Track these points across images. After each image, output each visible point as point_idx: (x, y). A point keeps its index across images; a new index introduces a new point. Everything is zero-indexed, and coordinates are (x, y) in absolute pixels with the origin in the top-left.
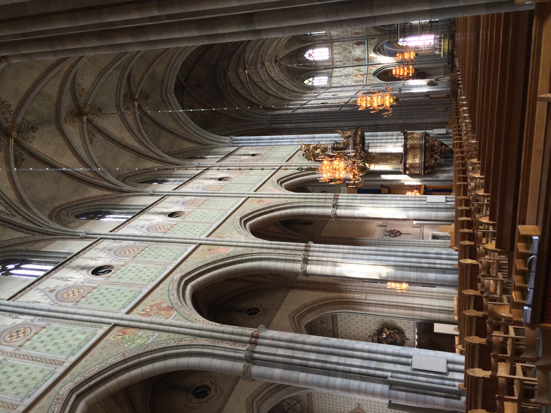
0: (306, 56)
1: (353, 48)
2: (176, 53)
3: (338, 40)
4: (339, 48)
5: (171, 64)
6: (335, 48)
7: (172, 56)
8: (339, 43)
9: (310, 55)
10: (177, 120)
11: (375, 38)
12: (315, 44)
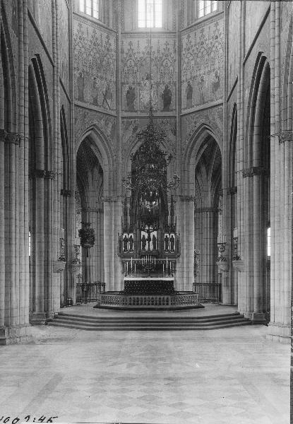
11: (175, 134)
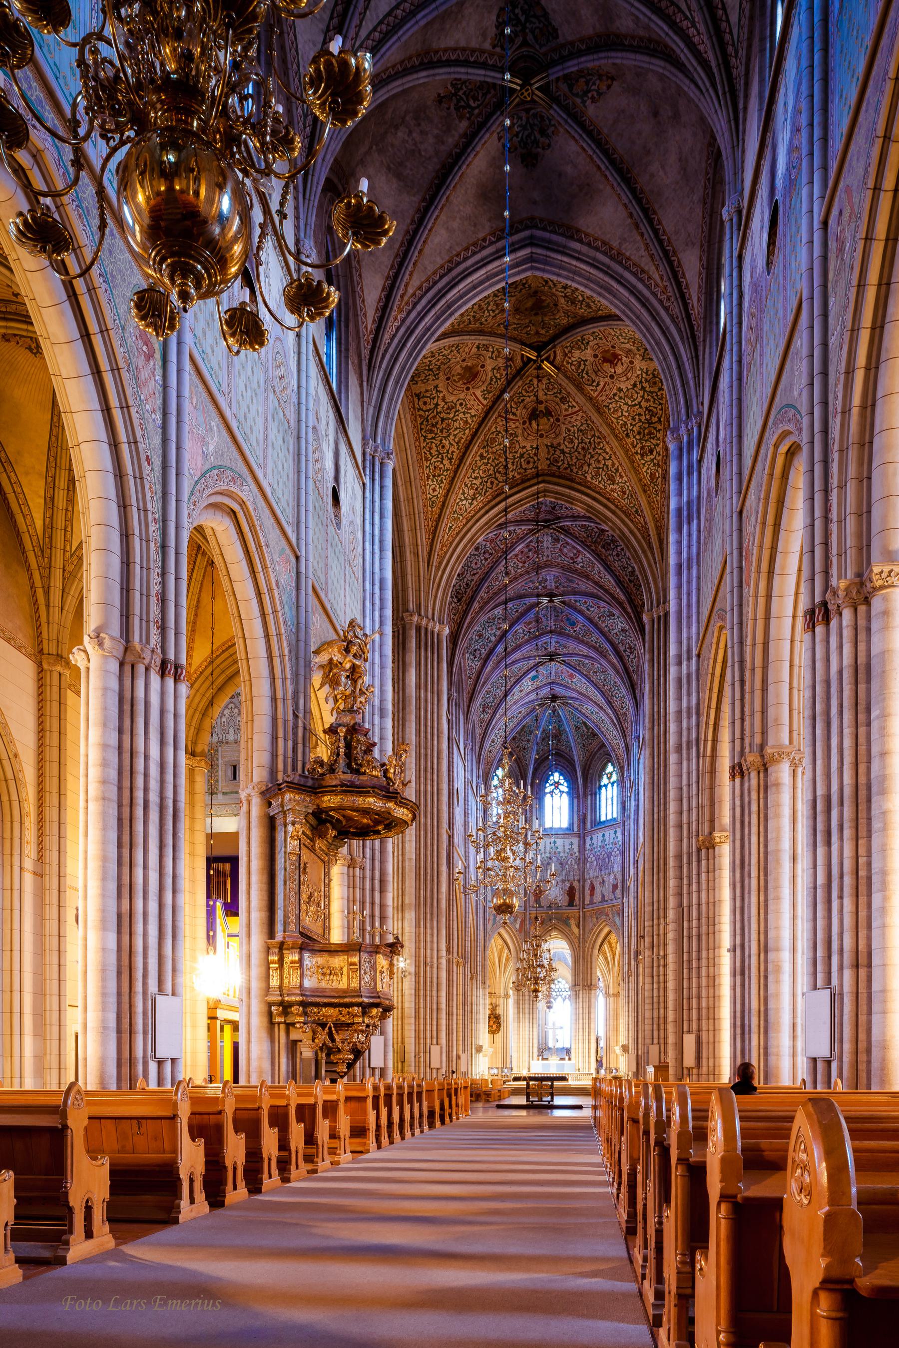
0: (556, 776)
1: (563, 881)
2: (648, 287)
3: (582, 848)
4: (567, 850)
5: (620, 269)
6: (567, 841)
7: (643, 271)
8: (576, 850)
9: (557, 784)
10: (450, 270)
12: (578, 797)
